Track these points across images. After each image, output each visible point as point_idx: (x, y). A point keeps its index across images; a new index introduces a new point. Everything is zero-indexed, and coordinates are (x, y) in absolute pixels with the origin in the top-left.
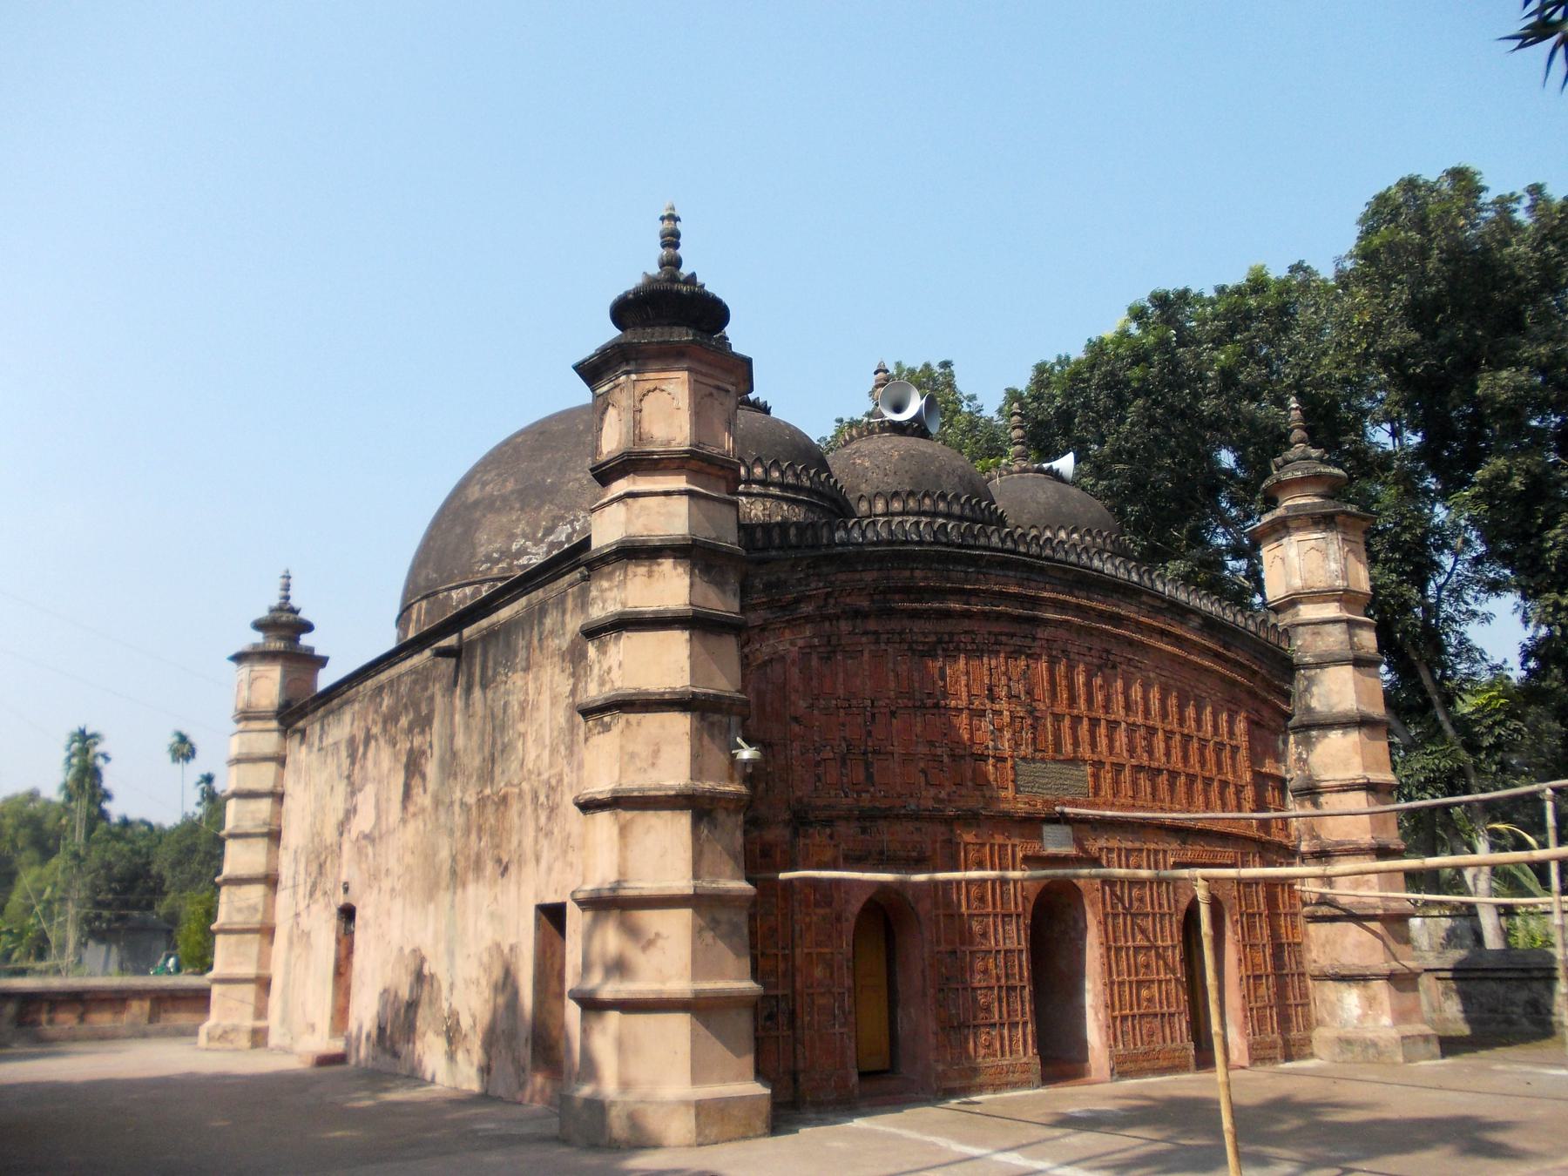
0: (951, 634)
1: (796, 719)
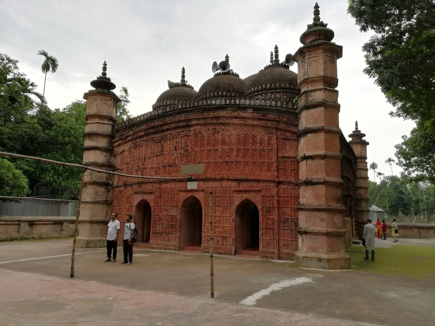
0: (166, 135)
1: (126, 163)
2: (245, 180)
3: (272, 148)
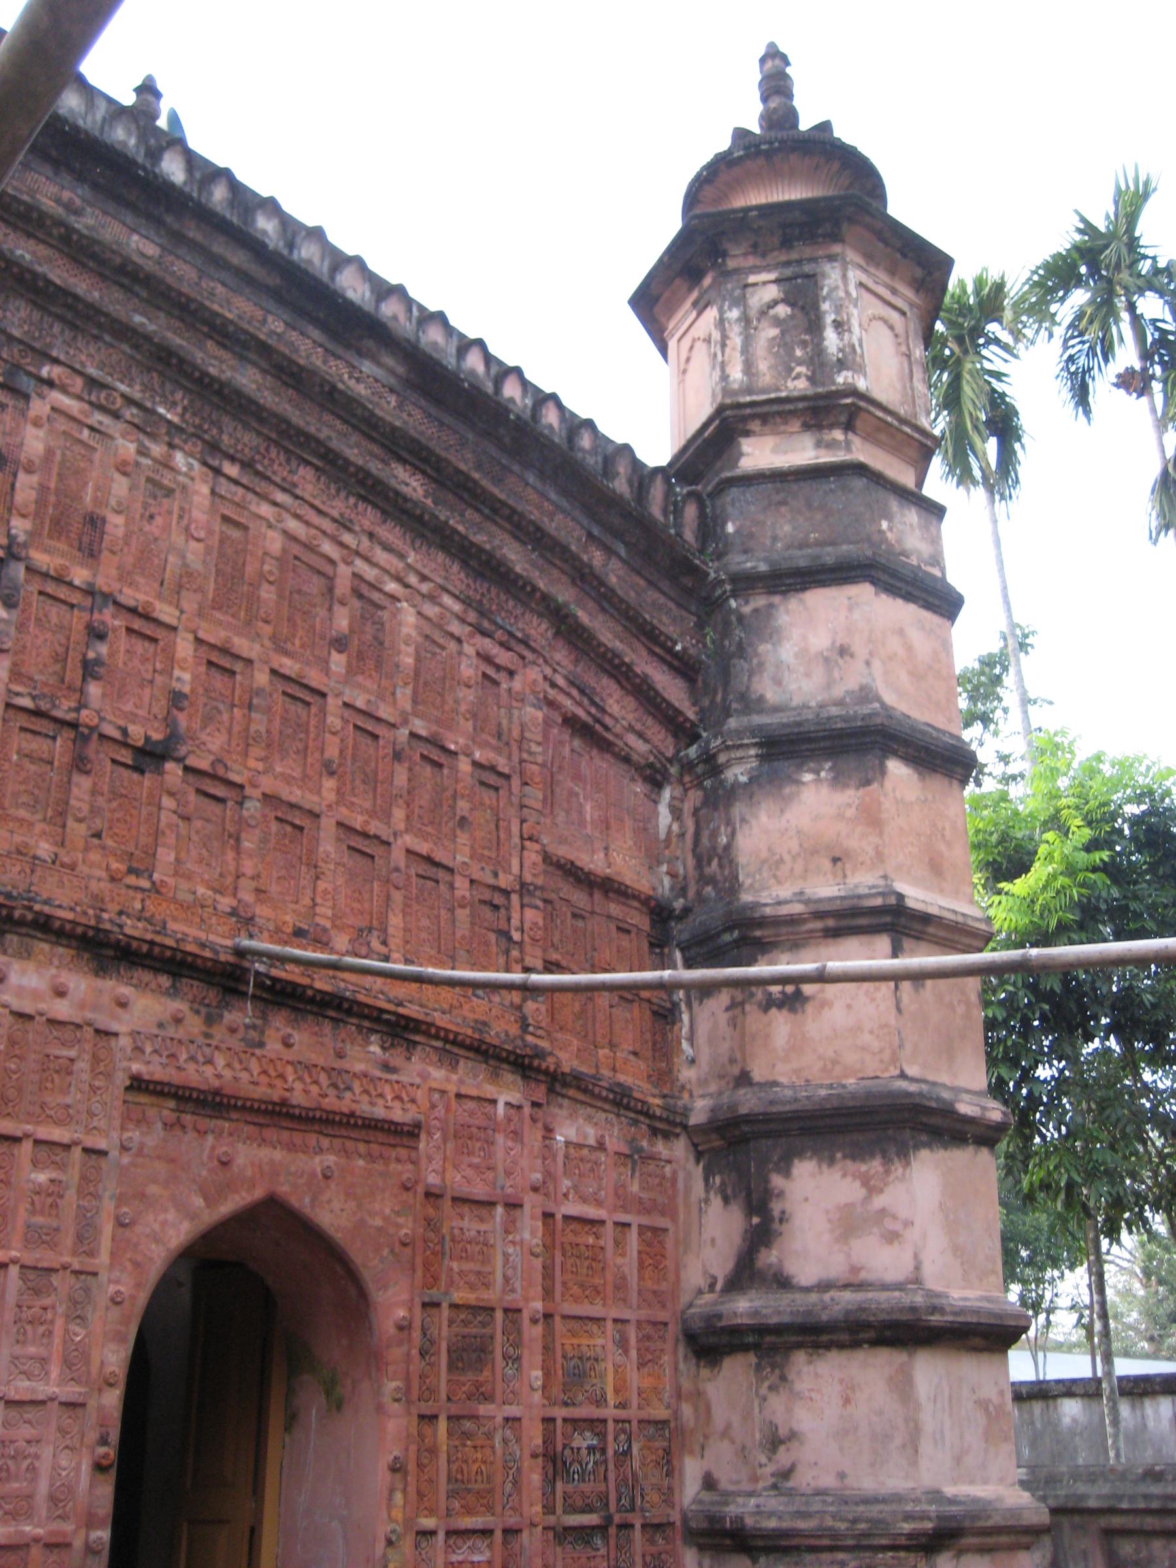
3: (503, 765)
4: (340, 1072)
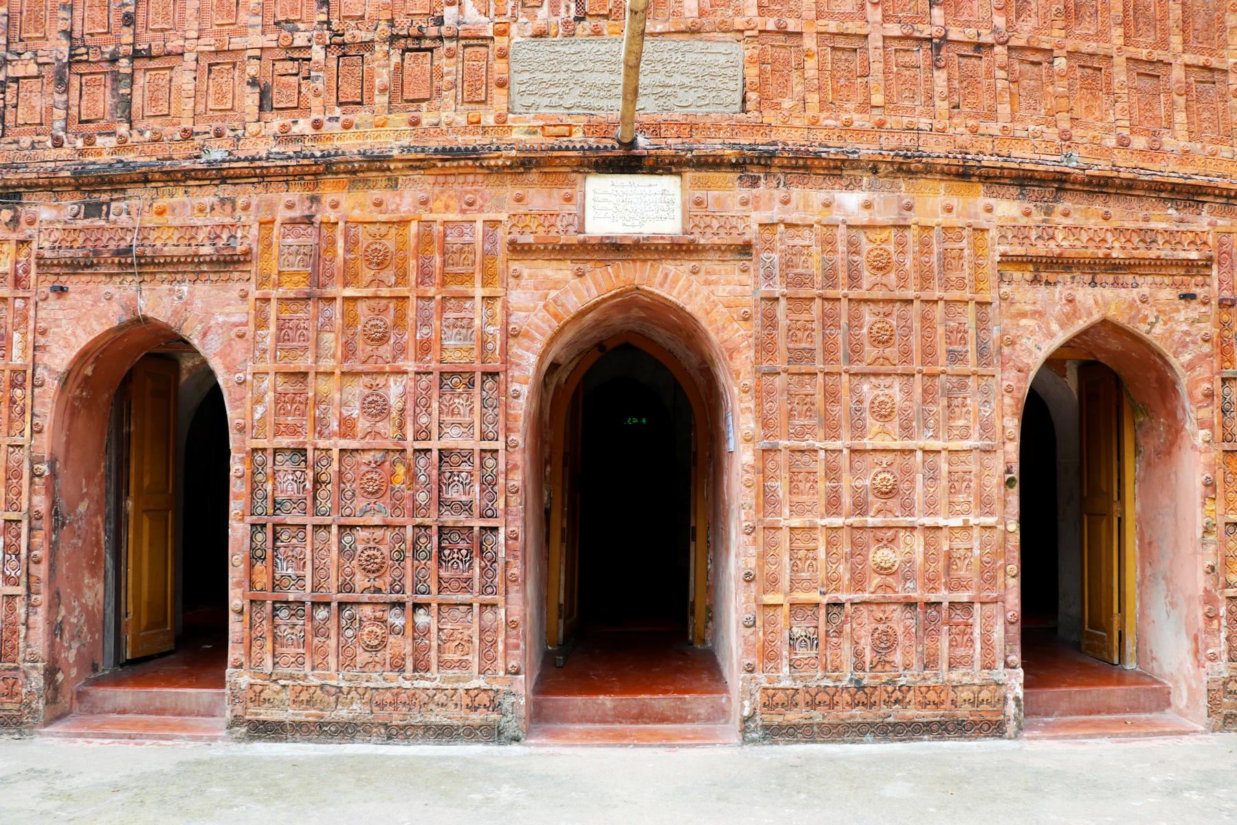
2: (1100, 187)
4: (1146, 231)
